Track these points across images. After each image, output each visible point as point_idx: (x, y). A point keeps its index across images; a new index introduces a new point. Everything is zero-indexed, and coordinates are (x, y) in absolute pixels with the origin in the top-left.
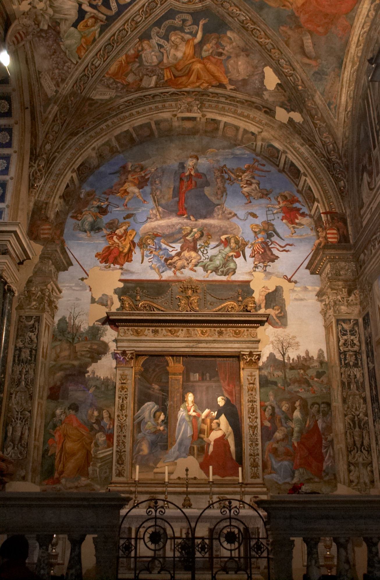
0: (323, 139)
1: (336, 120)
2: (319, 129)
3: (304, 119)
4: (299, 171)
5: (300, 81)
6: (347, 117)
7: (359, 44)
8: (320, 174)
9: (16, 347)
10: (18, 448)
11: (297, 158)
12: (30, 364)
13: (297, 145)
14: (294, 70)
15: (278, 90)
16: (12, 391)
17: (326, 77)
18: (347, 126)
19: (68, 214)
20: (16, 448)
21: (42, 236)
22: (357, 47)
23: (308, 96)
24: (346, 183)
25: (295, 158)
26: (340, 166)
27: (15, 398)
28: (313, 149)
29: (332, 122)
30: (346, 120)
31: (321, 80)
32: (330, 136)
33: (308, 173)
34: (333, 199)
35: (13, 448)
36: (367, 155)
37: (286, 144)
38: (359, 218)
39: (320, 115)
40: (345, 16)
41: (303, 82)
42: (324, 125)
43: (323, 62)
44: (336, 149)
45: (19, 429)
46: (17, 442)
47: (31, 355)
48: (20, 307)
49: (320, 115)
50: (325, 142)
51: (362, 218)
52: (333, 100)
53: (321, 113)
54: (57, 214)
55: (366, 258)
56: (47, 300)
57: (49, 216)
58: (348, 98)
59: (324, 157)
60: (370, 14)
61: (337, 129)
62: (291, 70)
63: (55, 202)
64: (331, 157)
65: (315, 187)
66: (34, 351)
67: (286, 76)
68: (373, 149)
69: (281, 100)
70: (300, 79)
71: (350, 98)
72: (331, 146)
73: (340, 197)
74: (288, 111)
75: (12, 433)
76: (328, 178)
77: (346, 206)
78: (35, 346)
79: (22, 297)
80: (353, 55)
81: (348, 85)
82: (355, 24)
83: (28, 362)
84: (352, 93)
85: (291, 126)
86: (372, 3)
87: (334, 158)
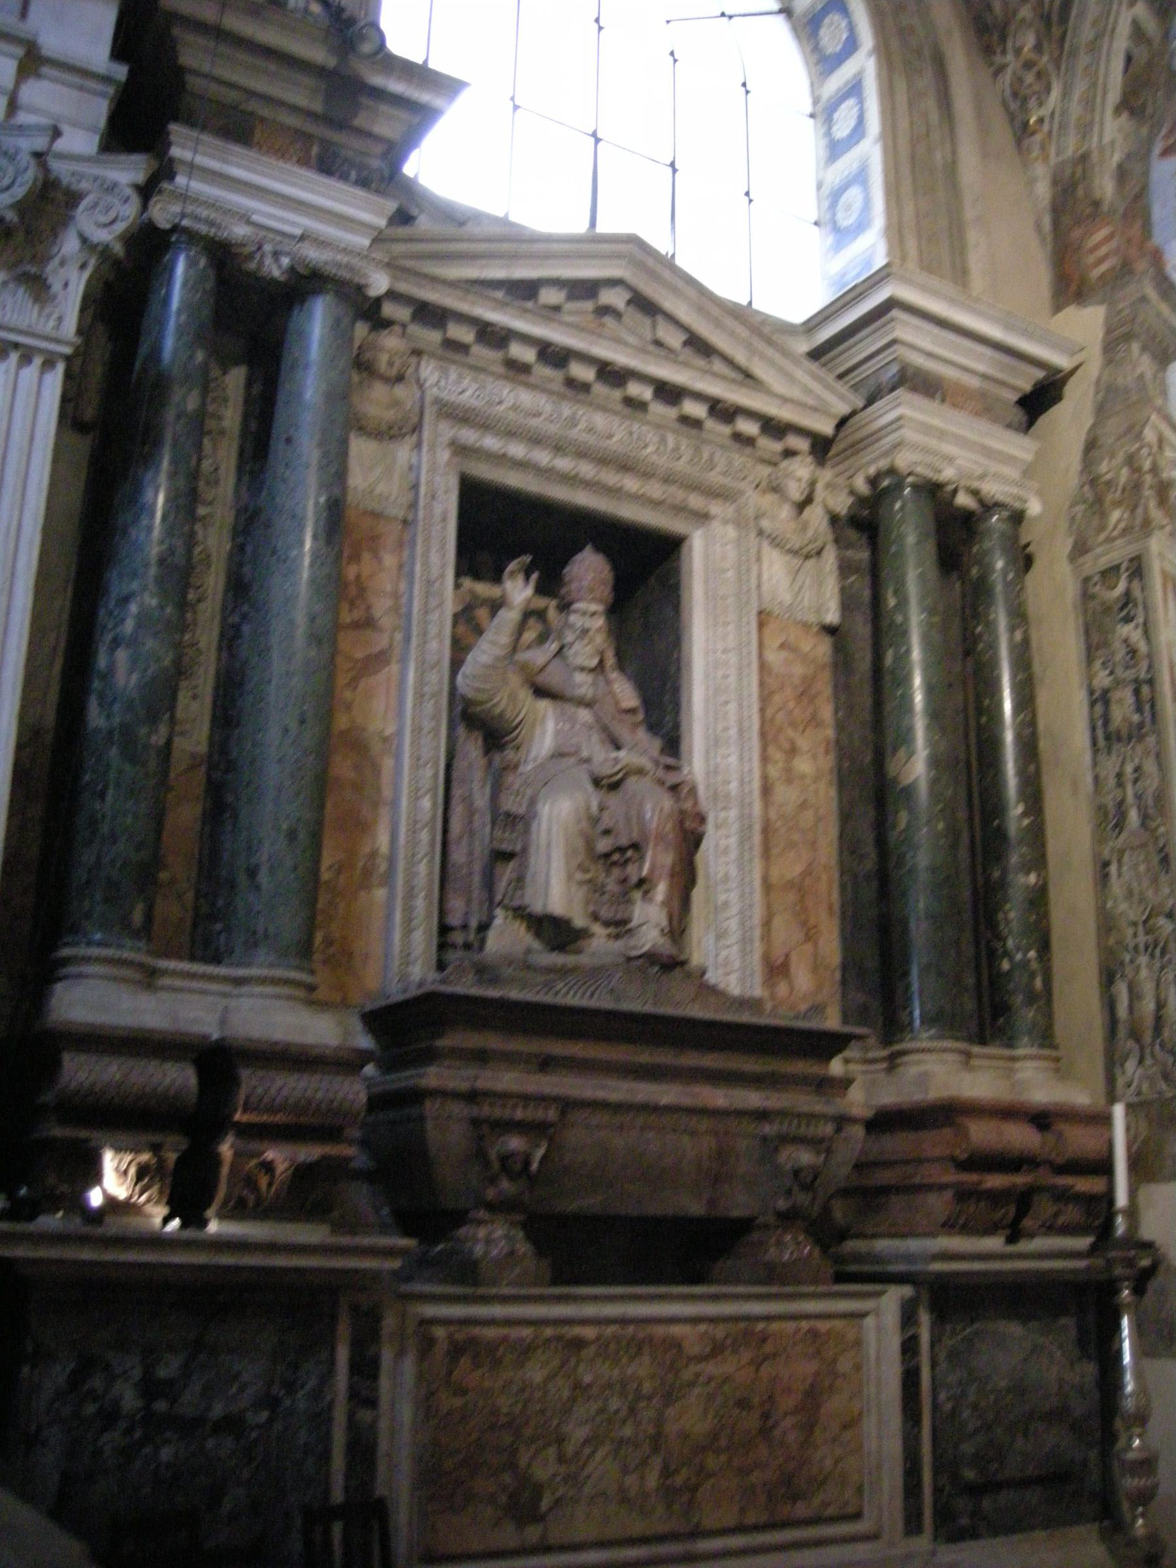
9: (1091, 692)
10: (1153, 1056)
12: (1141, 738)
16: (1106, 854)
19: (1149, 152)
20: (1148, 1061)
21: (1096, 273)
27: (1120, 875)
35: (1141, 1061)
45: (1148, 988)
46: (1148, 1037)
47: (1139, 709)
48: (1080, 549)
54: (1122, 174)
56: (1151, 487)
57: (1097, 195)
63: (1106, 139)
66: (1145, 690)
75: (1131, 1008)
78: (1145, 668)
79: (1080, 508)
83: (1136, 734)
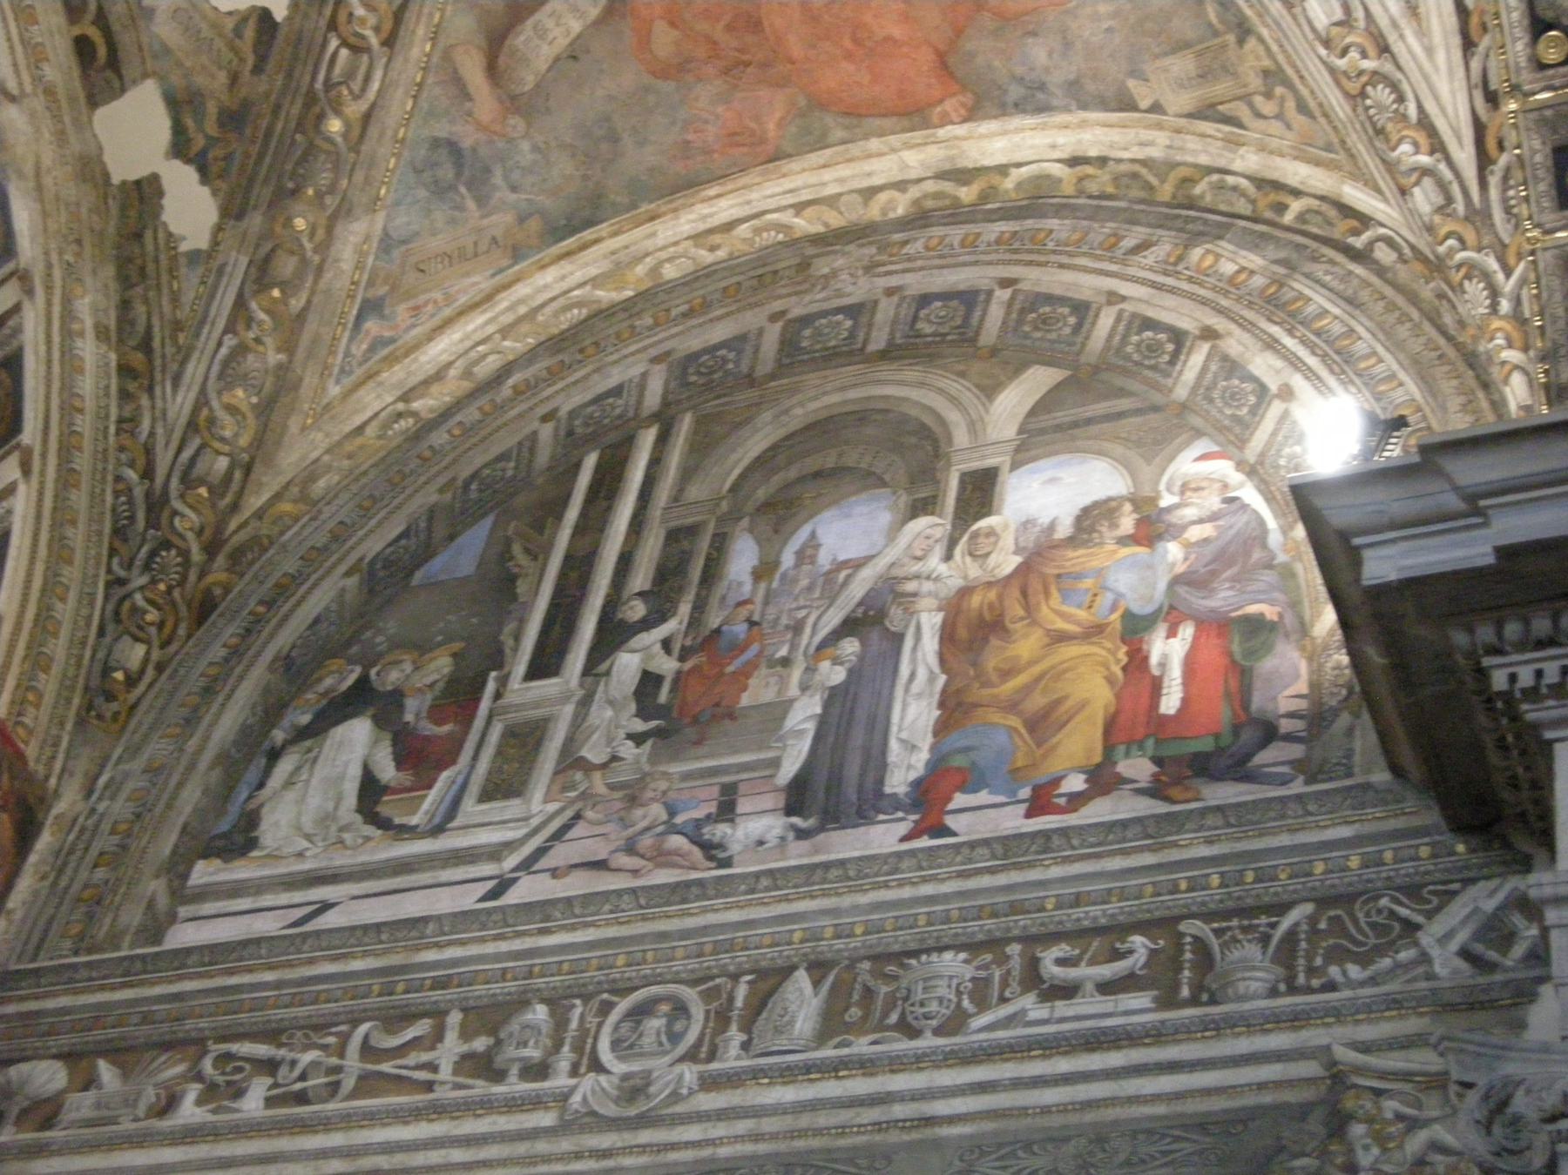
0: (215, 404)
1: (334, 390)
2: (241, 350)
3: (215, 243)
4: (15, 424)
5: (363, 106)
6: (386, 426)
7: (717, 239)
8: (73, 523)
11: (49, 362)
13: (84, 306)
14: (389, 42)
15: (238, 32)
17: (471, 204)
18: (350, 456)
22: (697, 238)
23: (332, 189)
24: (150, 673)
25: (43, 348)
26: (182, 583)
28: (125, 395)
29: (310, 380)
30: (370, 431)
31: (441, 190)
32: (251, 421)
33: (43, 473)
34: (49, 684)
36: (441, 665)
37: (54, 258)
38: (156, 887)
39: (296, 304)
40: (802, 102)
41: (367, 117)
42: (274, 358)
43: (525, 146)
44: (228, 499)
49: (296, 304)
50: (212, 421)
51: (181, 894)
52: (402, 311)
53: (309, 302)
55: (81, 1105)
58: (460, 364)
59: (148, 473)
60: (883, 197)
61: (304, 429)
62: (377, 29)
64: (177, 505)
65: (24, 562)
67: (333, 26)
68: (521, 668)
69: (200, 80)
70: (372, 93)
71: (467, 374)
72: (222, 463)
73: (76, 701)
74: (180, 148)
76: (91, 572)
77: (82, 765)
80: (649, 244)
81: (508, 318)
82: (795, 165)
84: (493, 363)
85: (123, 209)
86: (941, 176)
87: (187, 520)
